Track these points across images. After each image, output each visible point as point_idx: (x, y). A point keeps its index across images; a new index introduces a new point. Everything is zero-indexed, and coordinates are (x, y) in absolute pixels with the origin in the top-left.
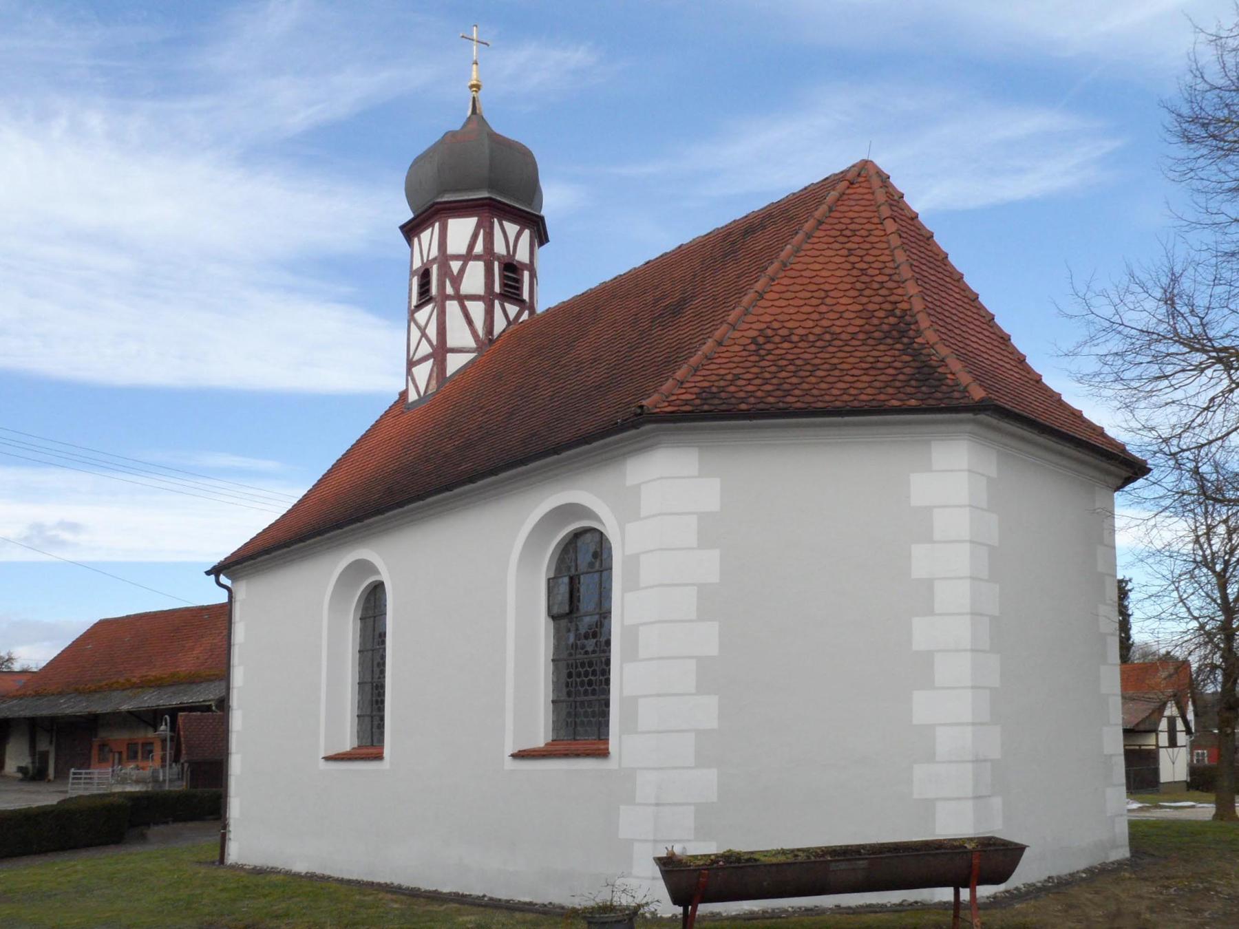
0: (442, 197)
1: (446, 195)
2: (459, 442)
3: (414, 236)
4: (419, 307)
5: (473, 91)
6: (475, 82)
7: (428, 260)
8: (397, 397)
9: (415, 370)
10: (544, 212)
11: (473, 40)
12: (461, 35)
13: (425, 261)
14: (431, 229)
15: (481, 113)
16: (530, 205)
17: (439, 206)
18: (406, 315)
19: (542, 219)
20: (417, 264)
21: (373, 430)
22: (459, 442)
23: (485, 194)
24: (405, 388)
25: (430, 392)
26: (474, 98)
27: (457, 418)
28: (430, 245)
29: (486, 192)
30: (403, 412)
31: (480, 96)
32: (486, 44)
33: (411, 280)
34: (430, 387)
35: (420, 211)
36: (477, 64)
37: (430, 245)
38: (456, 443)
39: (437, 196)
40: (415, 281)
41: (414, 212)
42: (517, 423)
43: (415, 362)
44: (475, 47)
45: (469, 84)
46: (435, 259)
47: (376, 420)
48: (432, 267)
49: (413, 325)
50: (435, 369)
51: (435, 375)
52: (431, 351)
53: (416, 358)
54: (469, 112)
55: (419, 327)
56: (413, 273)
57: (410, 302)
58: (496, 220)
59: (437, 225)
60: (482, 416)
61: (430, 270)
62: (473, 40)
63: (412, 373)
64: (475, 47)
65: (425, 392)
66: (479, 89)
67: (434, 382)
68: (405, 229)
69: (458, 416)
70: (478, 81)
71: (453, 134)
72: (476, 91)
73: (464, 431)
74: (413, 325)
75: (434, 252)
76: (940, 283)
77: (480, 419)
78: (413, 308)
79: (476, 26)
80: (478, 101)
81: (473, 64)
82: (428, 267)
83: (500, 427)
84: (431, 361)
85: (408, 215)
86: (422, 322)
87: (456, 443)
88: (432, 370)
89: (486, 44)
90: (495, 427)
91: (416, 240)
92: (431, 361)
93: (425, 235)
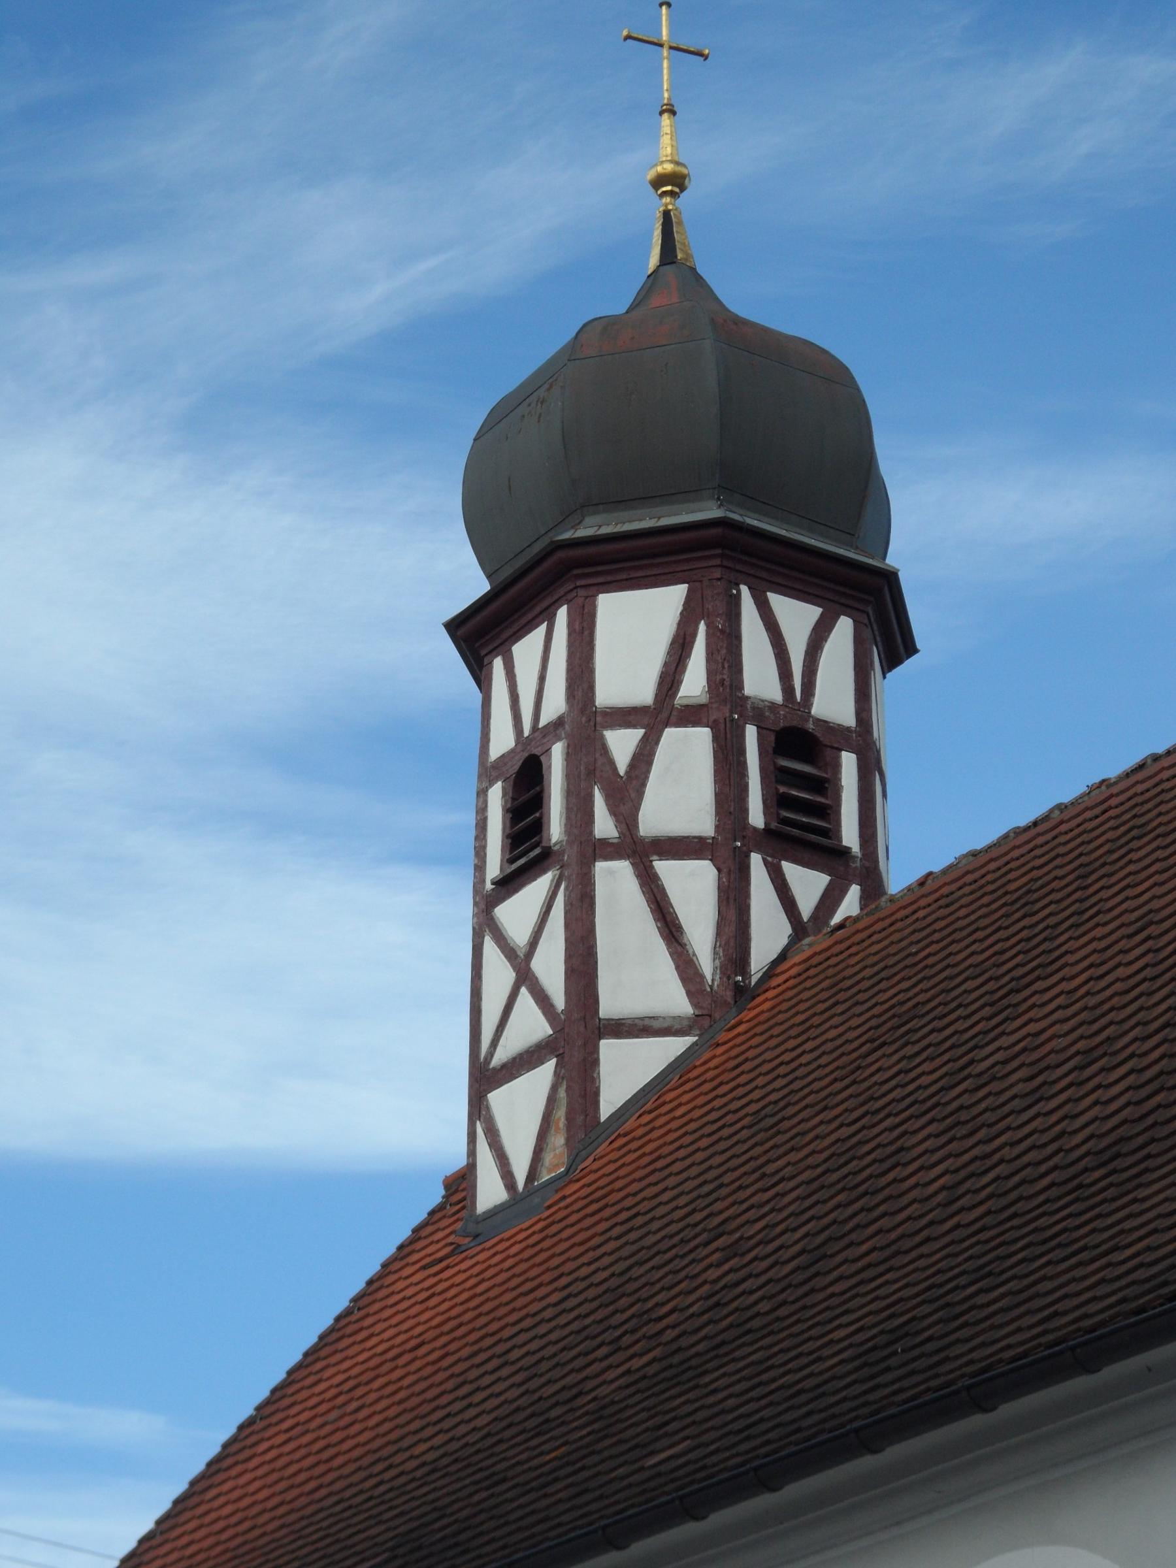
0: (575, 527)
1: (589, 520)
2: (645, 1359)
3: (494, 652)
4: (509, 884)
5: (665, 193)
6: (669, 167)
7: (535, 728)
8: (436, 1195)
9: (497, 1098)
10: (894, 559)
11: (661, 45)
12: (625, 33)
13: (527, 732)
14: (542, 630)
15: (688, 256)
16: (850, 535)
17: (561, 555)
18: (465, 910)
19: (891, 578)
20: (502, 741)
21: (357, 1315)
22: (645, 1359)
23: (711, 511)
24: (461, 1161)
25: (545, 1177)
26: (667, 215)
27: (636, 1272)
28: (542, 679)
29: (712, 504)
30: (457, 1249)
31: (685, 204)
32: (699, 54)
33: (482, 793)
34: (548, 1158)
35: (507, 573)
36: (673, 113)
37: (542, 679)
38: (636, 1363)
39: (558, 525)
40: (496, 795)
41: (489, 577)
42: (836, 1288)
43: (496, 1071)
44: (665, 64)
45: (651, 175)
46: (559, 723)
47: (398, 1242)
48: (548, 751)
49: (489, 946)
50: (562, 1093)
51: (561, 1114)
52: (551, 1032)
53: (501, 1055)
54: (654, 260)
55: (509, 951)
56: (488, 772)
57: (480, 868)
58: (745, 590)
59: (562, 614)
60: (719, 1264)
61: (543, 758)
62: (661, 45)
63: (488, 1108)
64: (665, 64)
65: (532, 1175)
66: (683, 188)
67: (558, 1141)
68: (461, 632)
69: (641, 1263)
70: (677, 163)
71: (605, 327)
72: (672, 194)
73: (660, 1319)
74: (489, 946)
75: (555, 703)
76: (1013, 873)
77: (713, 1274)
78: (489, 886)
79: (669, 5)
80: (680, 223)
81: (661, 113)
82: (537, 751)
83: (784, 1303)
84: (550, 1066)
85: (476, 585)
86: (519, 935)
87: (636, 1363)
88: (551, 1100)
89: (699, 54)
90: (764, 1306)
91: (498, 664)
92: (550, 1066)
93: (526, 651)
